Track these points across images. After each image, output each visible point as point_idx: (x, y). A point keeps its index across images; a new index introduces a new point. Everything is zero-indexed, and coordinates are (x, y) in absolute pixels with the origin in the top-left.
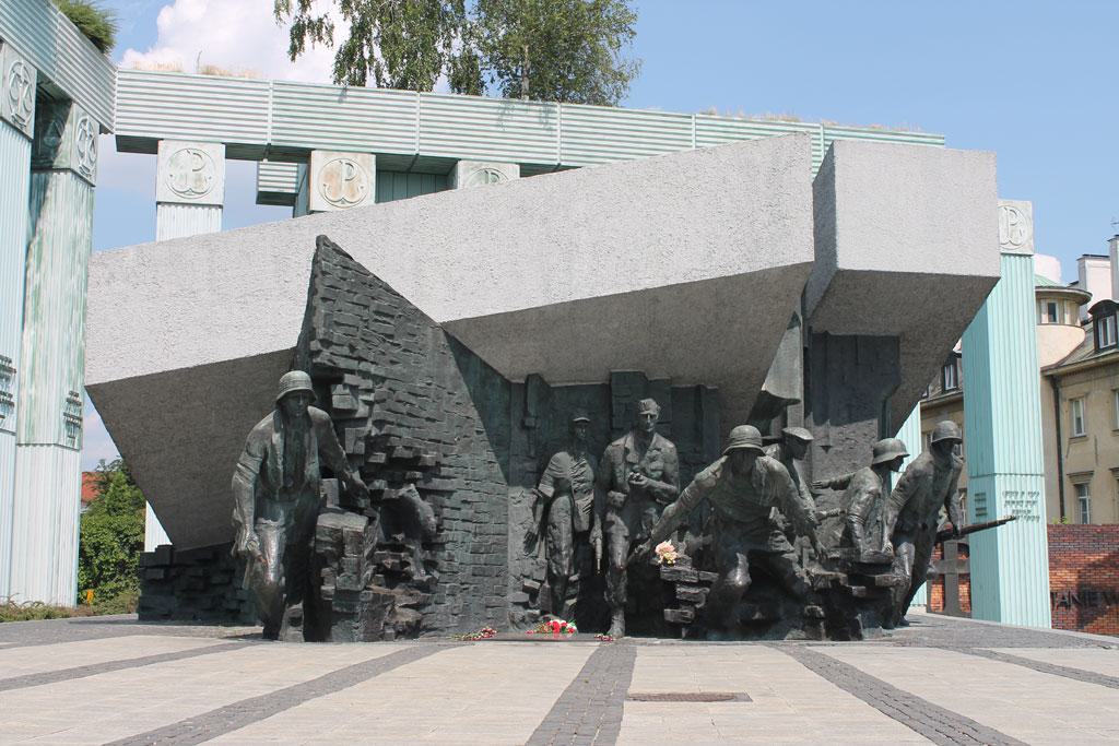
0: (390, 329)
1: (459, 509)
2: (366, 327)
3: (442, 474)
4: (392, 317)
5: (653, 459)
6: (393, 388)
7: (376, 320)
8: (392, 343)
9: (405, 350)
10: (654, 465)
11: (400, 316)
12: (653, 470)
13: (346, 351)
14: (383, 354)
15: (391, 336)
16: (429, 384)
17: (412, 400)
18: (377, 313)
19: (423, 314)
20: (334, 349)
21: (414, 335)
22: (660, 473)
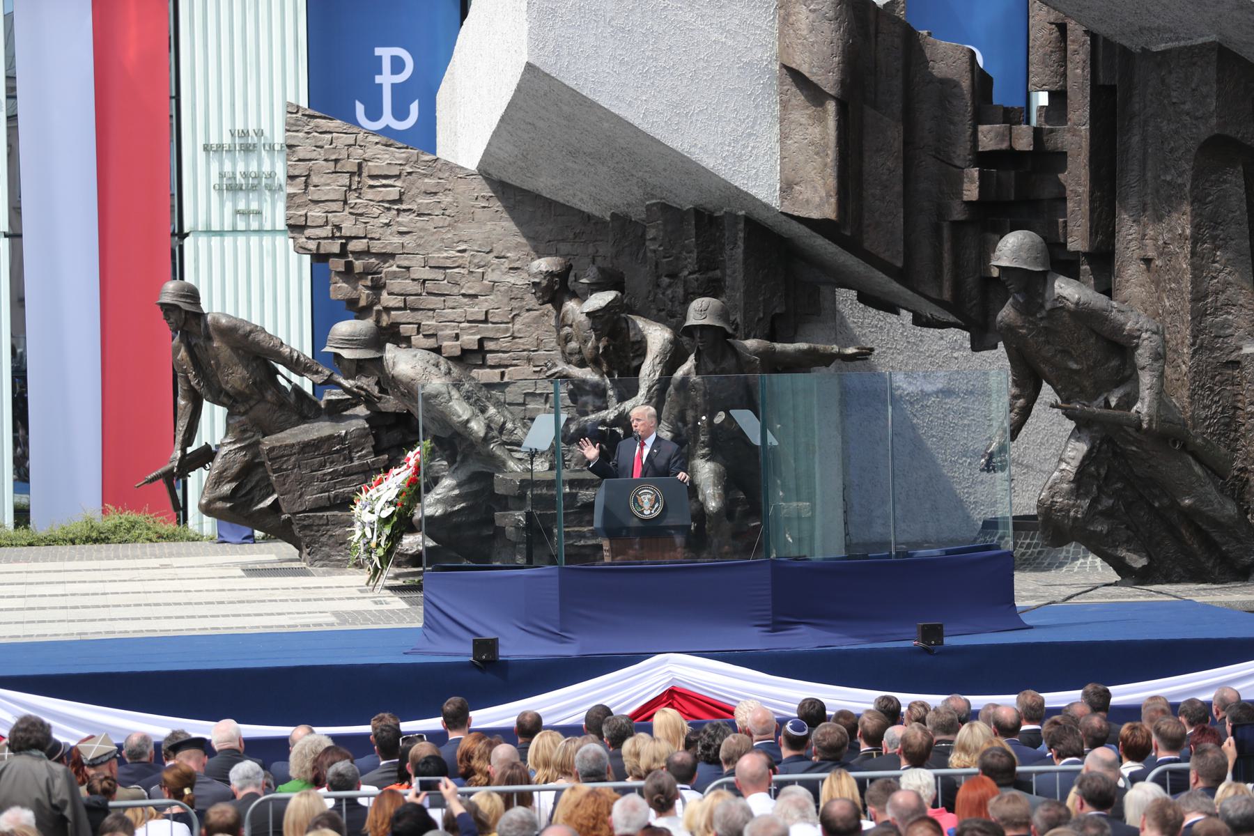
0: (393, 194)
1: (524, 404)
2: (358, 198)
3: (490, 362)
4: (398, 177)
6: (406, 263)
7: (371, 187)
8: (398, 210)
9: (419, 215)
11: (410, 173)
12: (570, 354)
13: (327, 231)
14: (388, 225)
15: (400, 201)
16: (464, 251)
17: (439, 275)
18: (372, 177)
20: (308, 232)
21: (435, 193)
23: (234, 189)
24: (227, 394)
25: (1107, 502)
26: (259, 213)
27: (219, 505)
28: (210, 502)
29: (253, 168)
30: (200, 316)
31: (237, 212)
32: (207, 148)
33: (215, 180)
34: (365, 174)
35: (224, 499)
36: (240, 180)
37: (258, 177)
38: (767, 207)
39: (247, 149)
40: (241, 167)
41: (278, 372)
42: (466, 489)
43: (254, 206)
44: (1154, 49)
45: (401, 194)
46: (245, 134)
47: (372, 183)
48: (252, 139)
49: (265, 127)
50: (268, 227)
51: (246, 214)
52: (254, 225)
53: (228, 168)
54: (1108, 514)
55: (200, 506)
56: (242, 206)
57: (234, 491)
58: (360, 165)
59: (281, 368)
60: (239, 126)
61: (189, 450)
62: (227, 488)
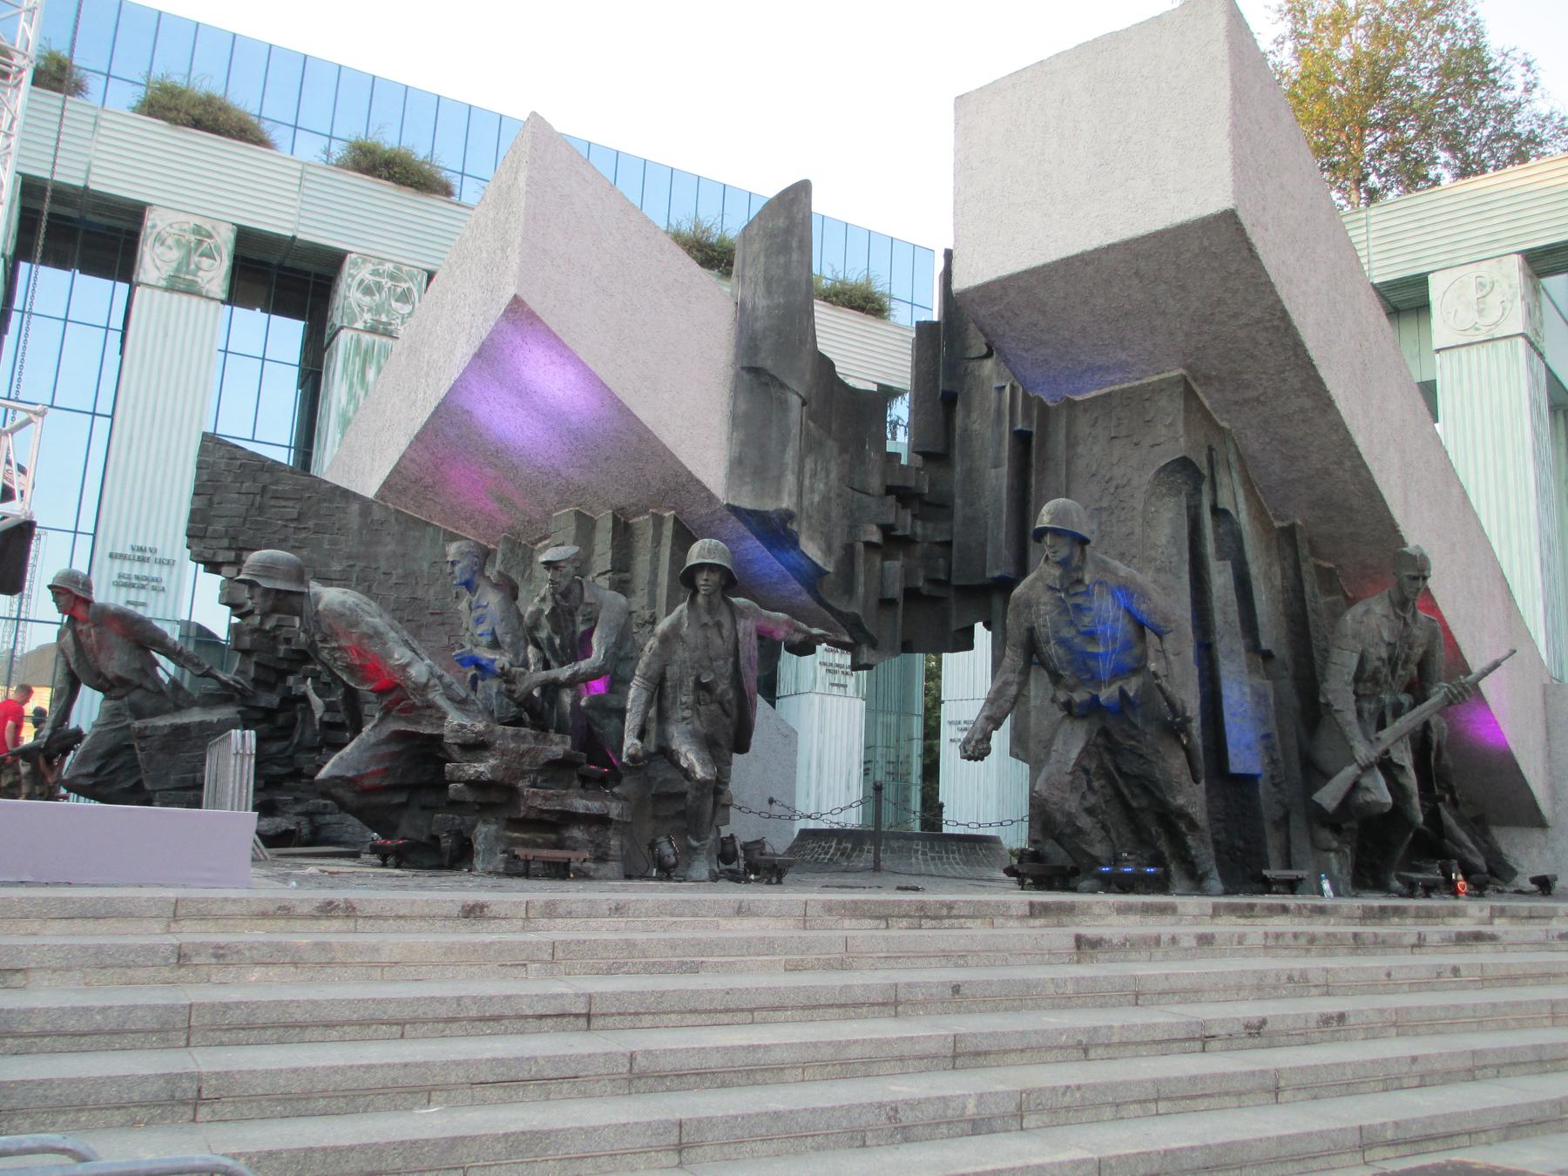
5: (479, 621)
10: (481, 629)
19: (346, 491)
22: (489, 638)
24: (105, 679)
25: (1092, 800)
27: (81, 781)
30: (88, 602)
32: (111, 556)
34: (269, 495)
35: (88, 775)
38: (711, 497)
39: (143, 560)
41: (156, 664)
42: (384, 749)
43: (142, 600)
44: (1078, 398)
45: (300, 514)
46: (141, 549)
47: (272, 502)
53: (126, 571)
54: (1090, 811)
57: (99, 770)
58: (264, 489)
59: (162, 660)
62: (92, 768)
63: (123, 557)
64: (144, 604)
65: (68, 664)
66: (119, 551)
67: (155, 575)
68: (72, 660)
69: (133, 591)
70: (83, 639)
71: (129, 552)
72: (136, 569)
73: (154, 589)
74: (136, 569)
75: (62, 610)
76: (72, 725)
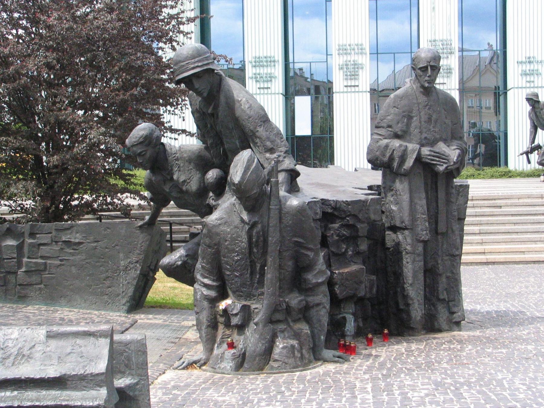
23: (526, 75)
26: (533, 82)
28: (541, 161)
29: (532, 68)
30: (538, 102)
31: (527, 81)
32: (518, 62)
33: (520, 72)
36: (528, 72)
37: (533, 71)
40: (528, 68)
43: (532, 79)
46: (529, 58)
48: (532, 59)
49: (536, 55)
50: (536, 86)
51: (529, 82)
52: (532, 85)
53: (524, 68)
55: (538, 162)
56: (528, 79)
60: (528, 56)
61: (533, 145)
63: (521, 62)
64: (533, 82)
65: (534, 123)
66: (520, 60)
67: (536, 68)
68: (535, 122)
69: (528, 77)
70: (538, 114)
71: (524, 60)
72: (527, 67)
73: (537, 75)
74: (527, 67)
75: (530, 105)
76: (536, 143)
